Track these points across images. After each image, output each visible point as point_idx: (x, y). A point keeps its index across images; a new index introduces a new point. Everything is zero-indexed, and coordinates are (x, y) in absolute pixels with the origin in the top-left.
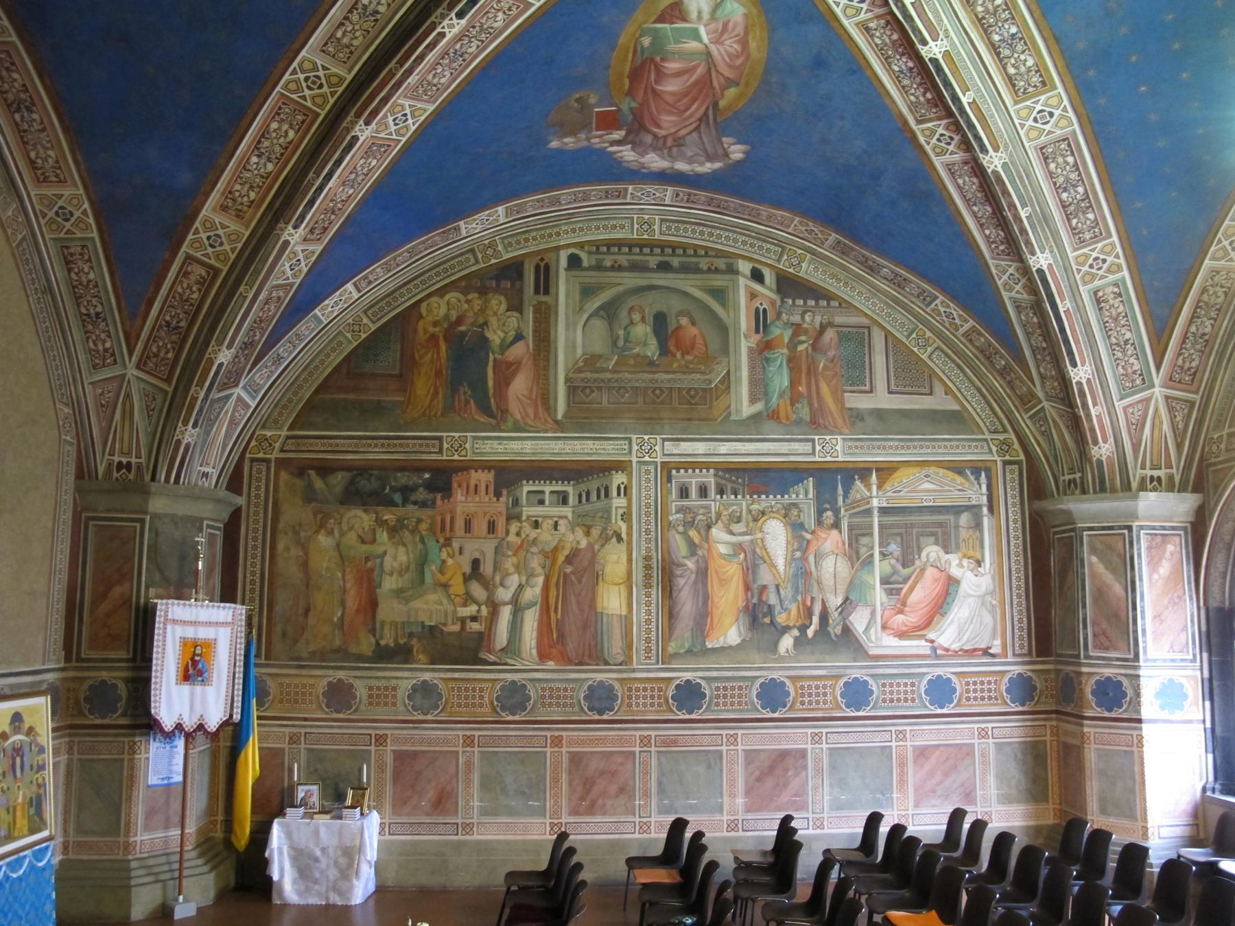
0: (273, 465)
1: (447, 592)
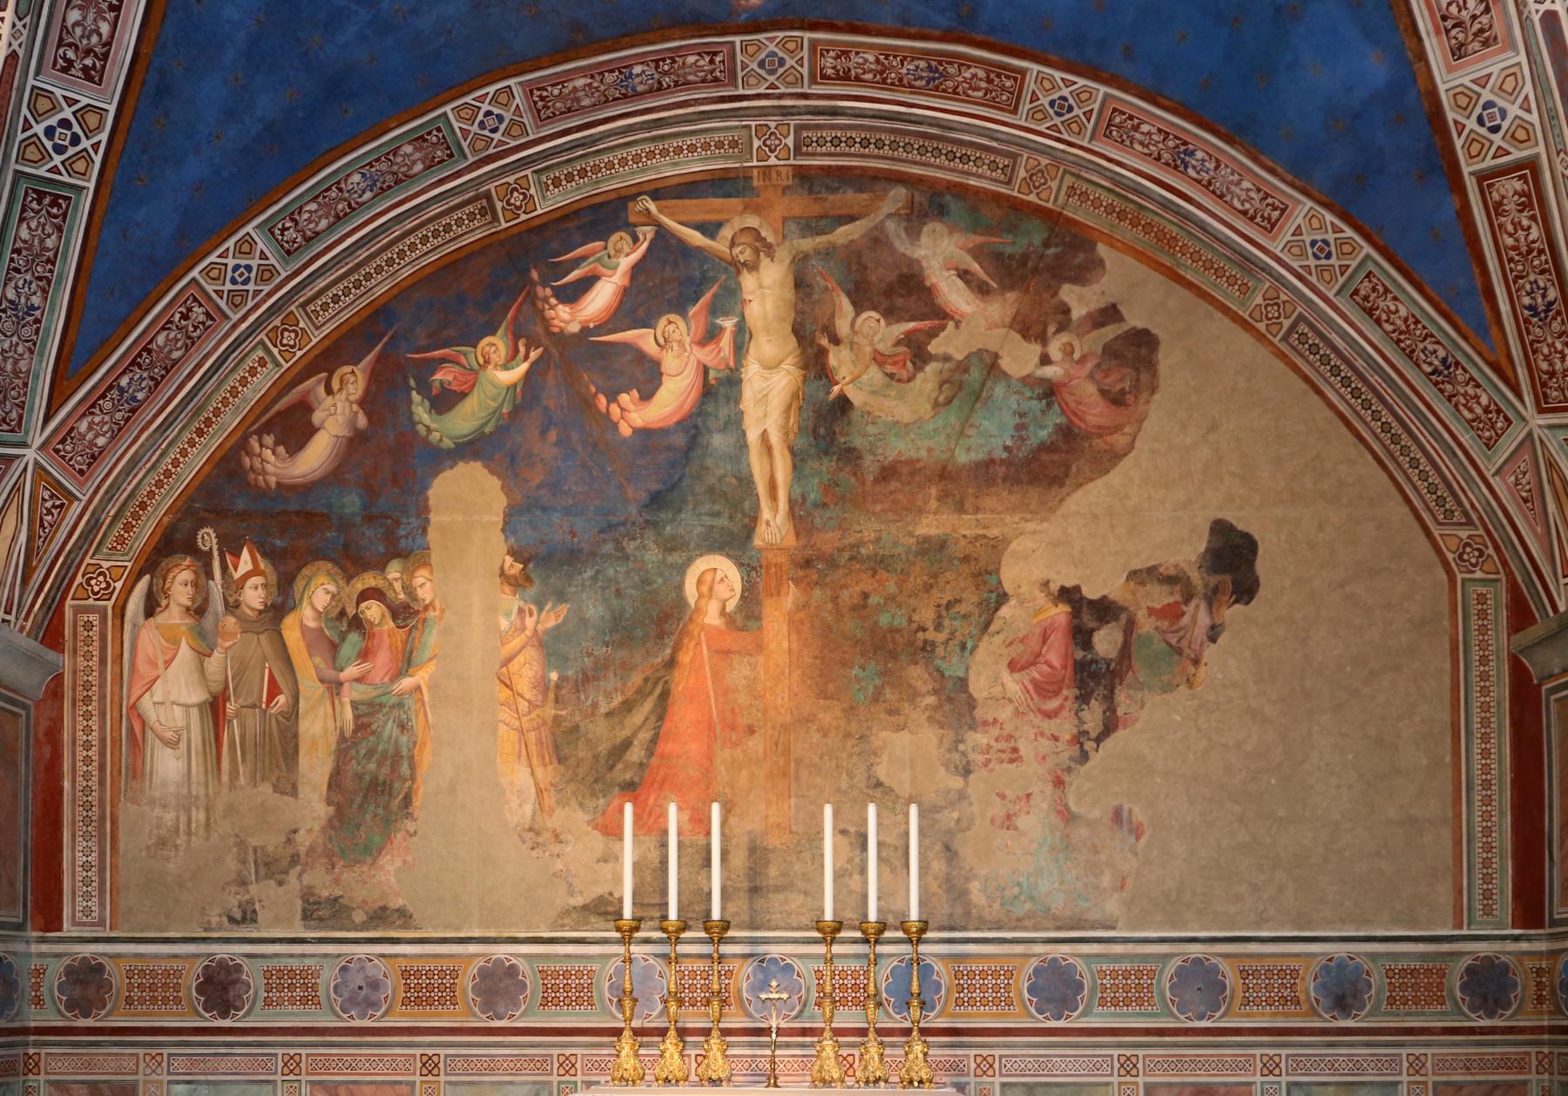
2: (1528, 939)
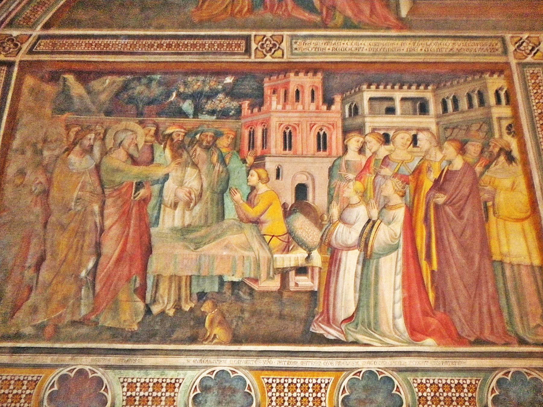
0: (16, 69)
1: (259, 231)
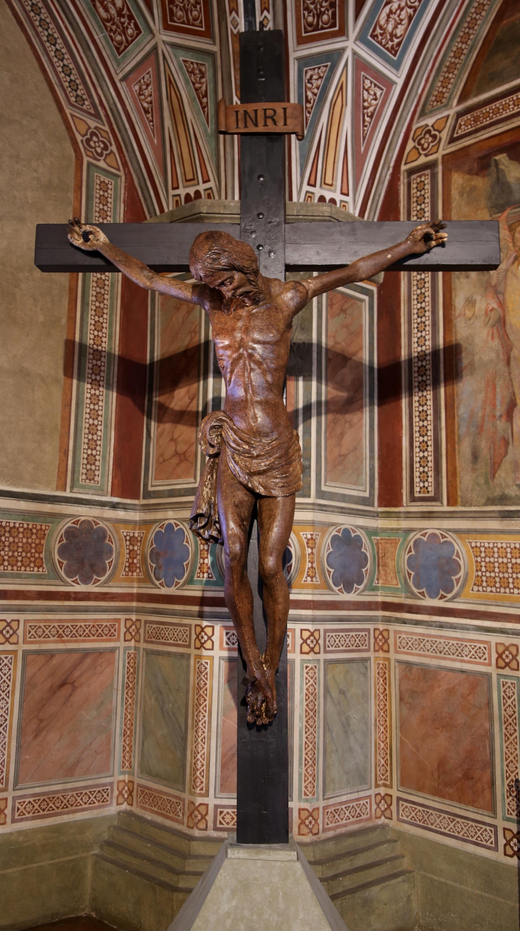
0: (440, 169)
2: (125, 507)
